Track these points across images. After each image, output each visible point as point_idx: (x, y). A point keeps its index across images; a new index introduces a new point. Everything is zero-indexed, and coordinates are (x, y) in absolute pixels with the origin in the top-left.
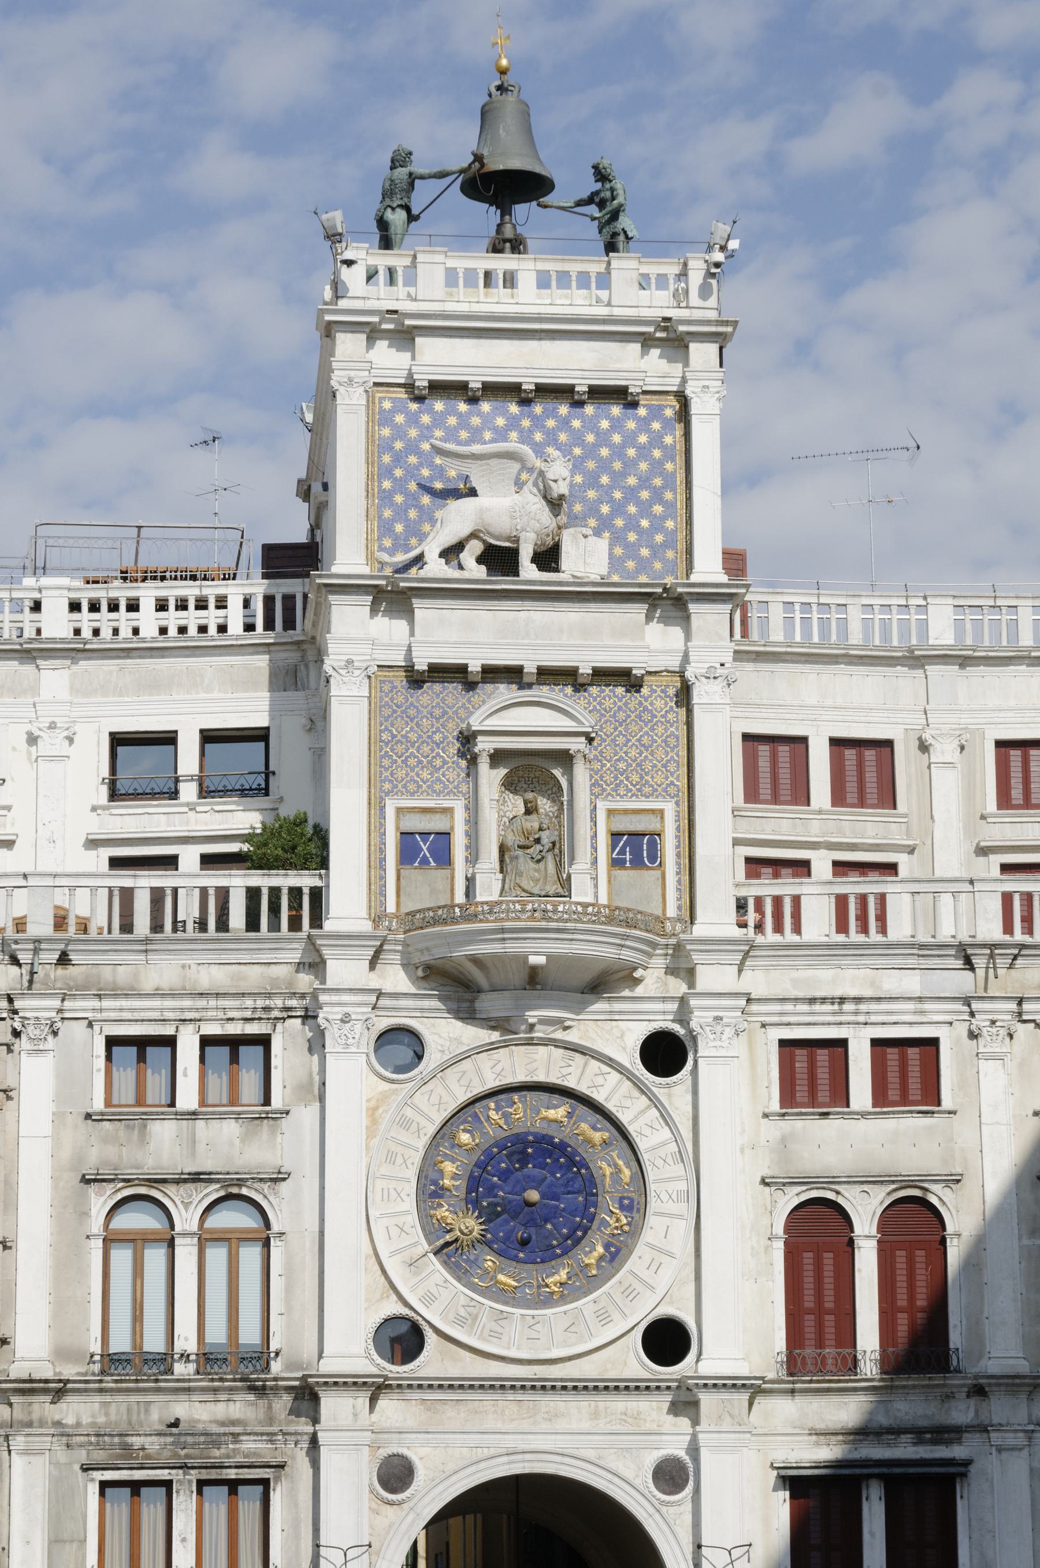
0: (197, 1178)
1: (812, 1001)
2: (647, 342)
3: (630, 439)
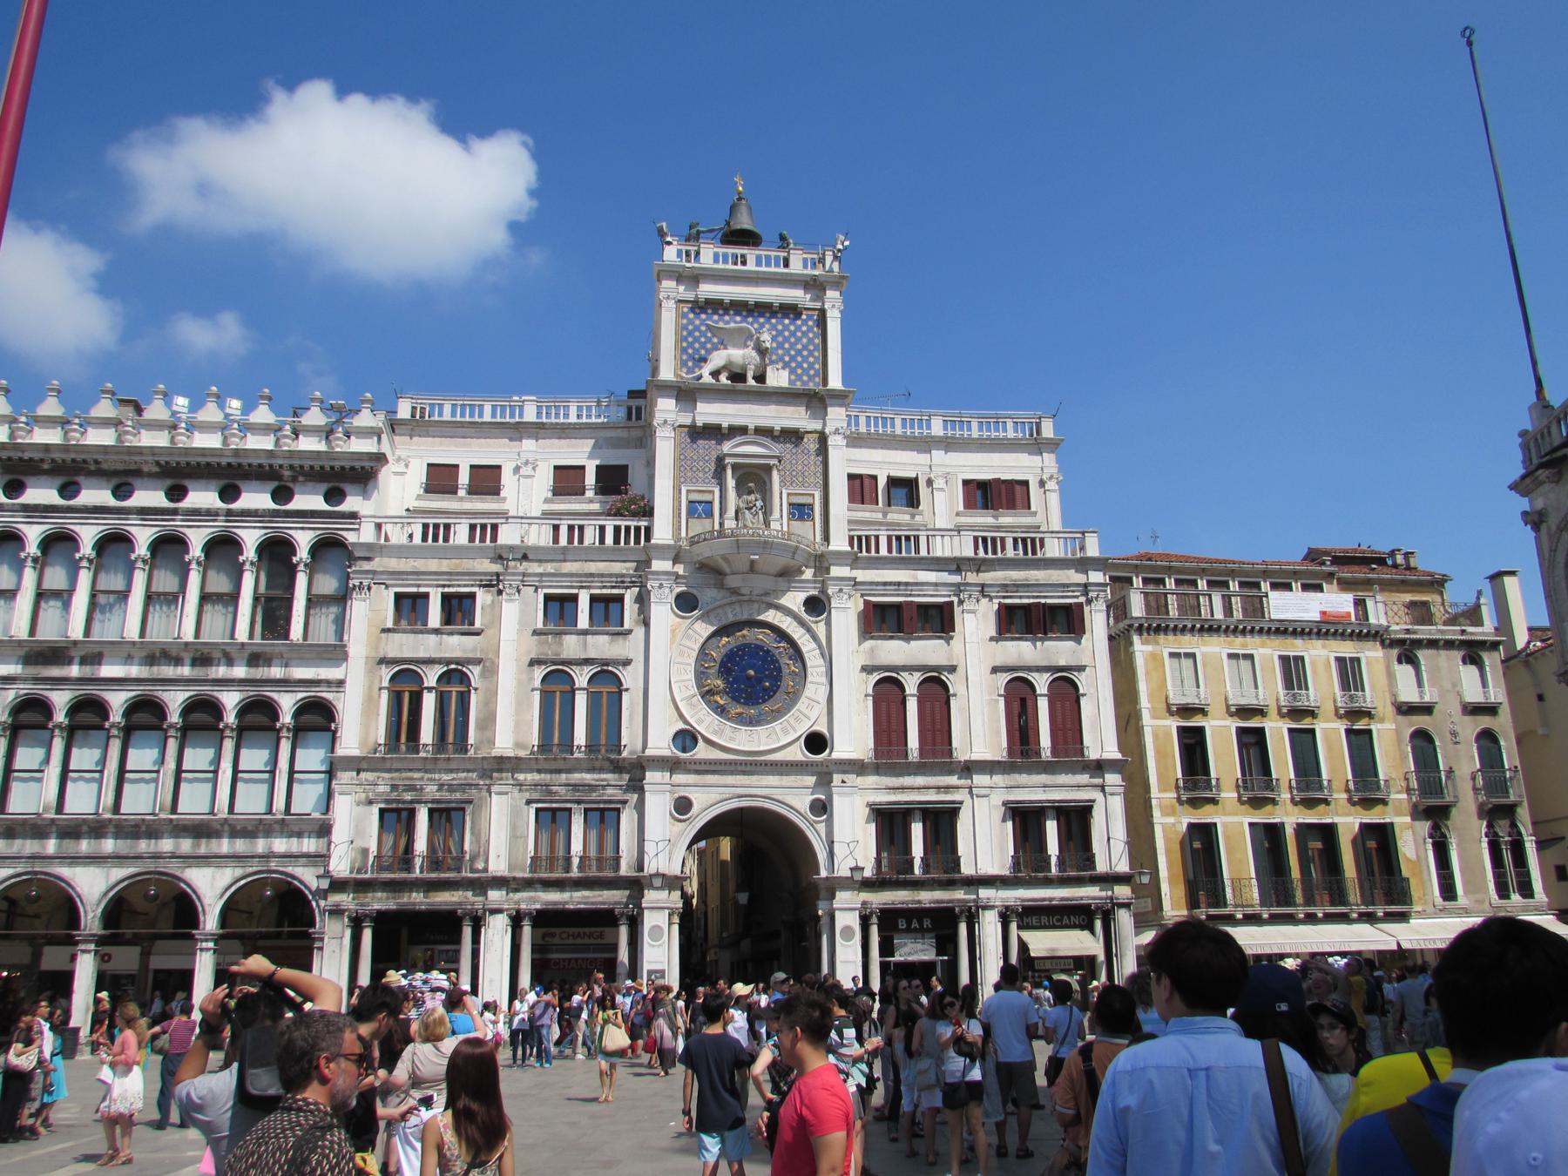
1: (885, 584)
3: (798, 328)
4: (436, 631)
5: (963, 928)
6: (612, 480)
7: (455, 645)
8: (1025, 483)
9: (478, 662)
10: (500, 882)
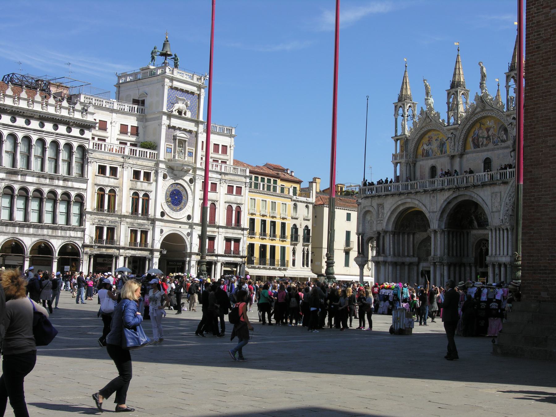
0: (143, 190)
2: (197, 87)
4: (108, 177)
5: (213, 266)
6: (136, 131)
7: (112, 182)
8: (226, 146)
9: (118, 187)
10: (123, 248)
